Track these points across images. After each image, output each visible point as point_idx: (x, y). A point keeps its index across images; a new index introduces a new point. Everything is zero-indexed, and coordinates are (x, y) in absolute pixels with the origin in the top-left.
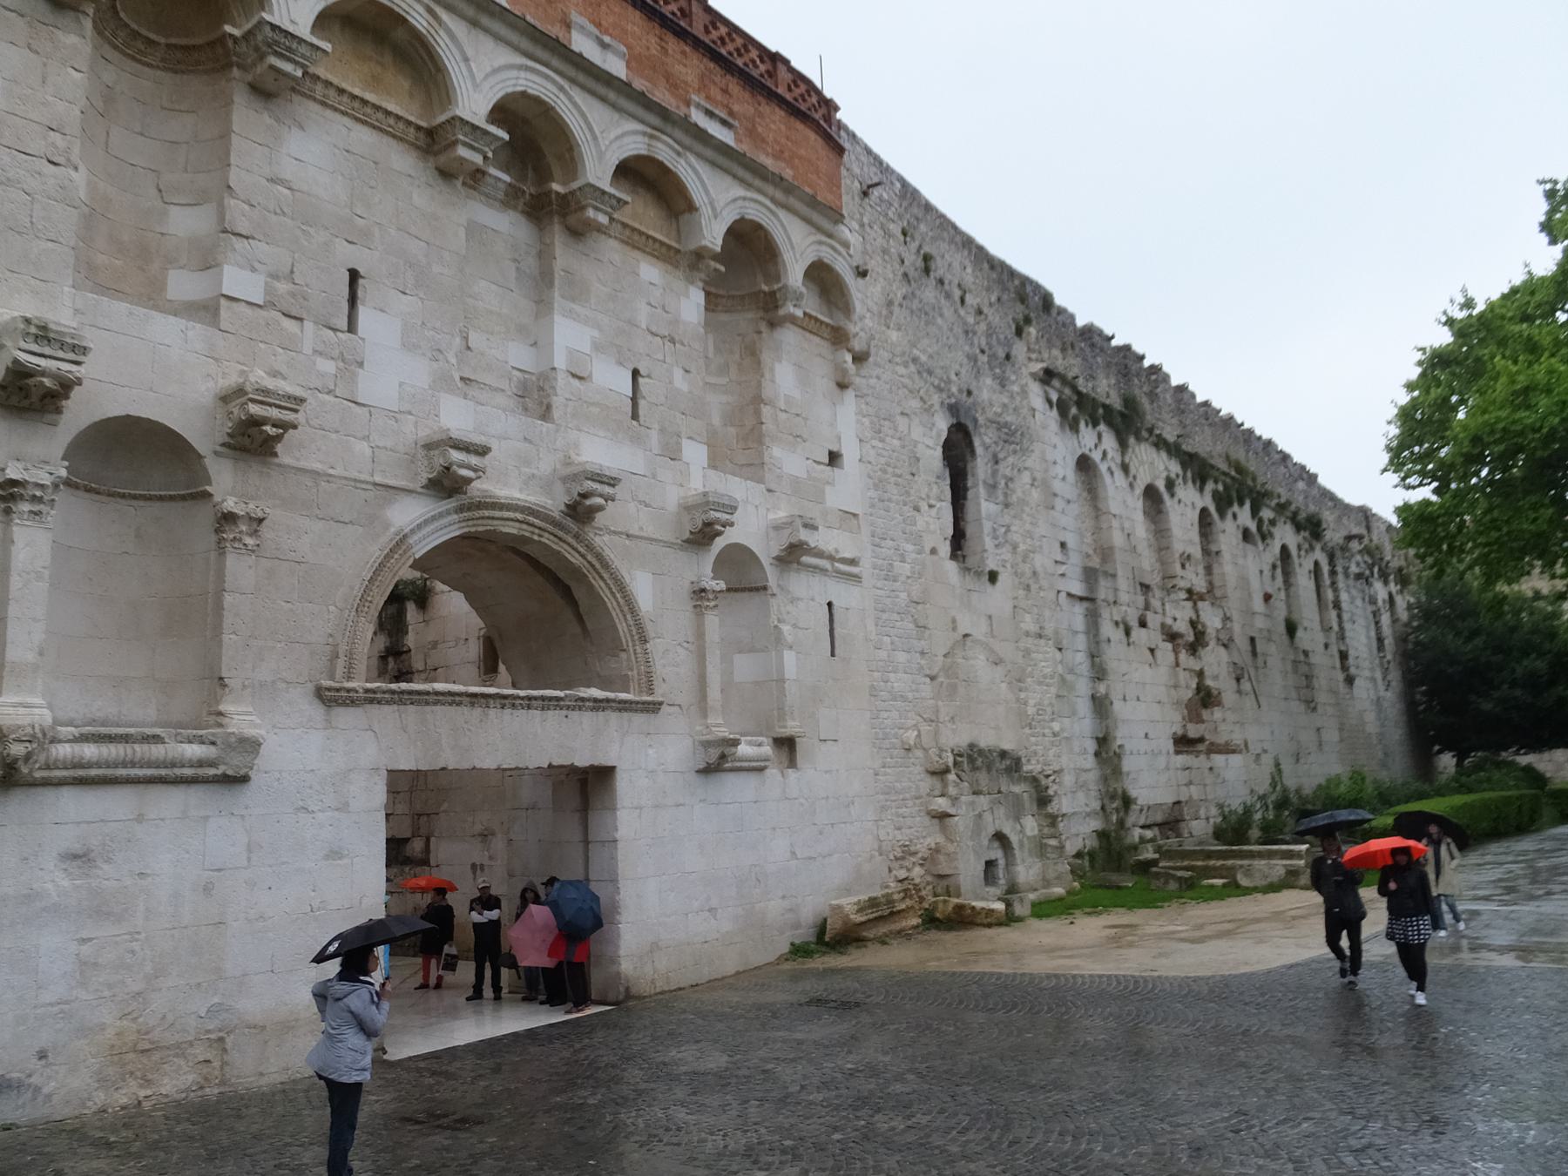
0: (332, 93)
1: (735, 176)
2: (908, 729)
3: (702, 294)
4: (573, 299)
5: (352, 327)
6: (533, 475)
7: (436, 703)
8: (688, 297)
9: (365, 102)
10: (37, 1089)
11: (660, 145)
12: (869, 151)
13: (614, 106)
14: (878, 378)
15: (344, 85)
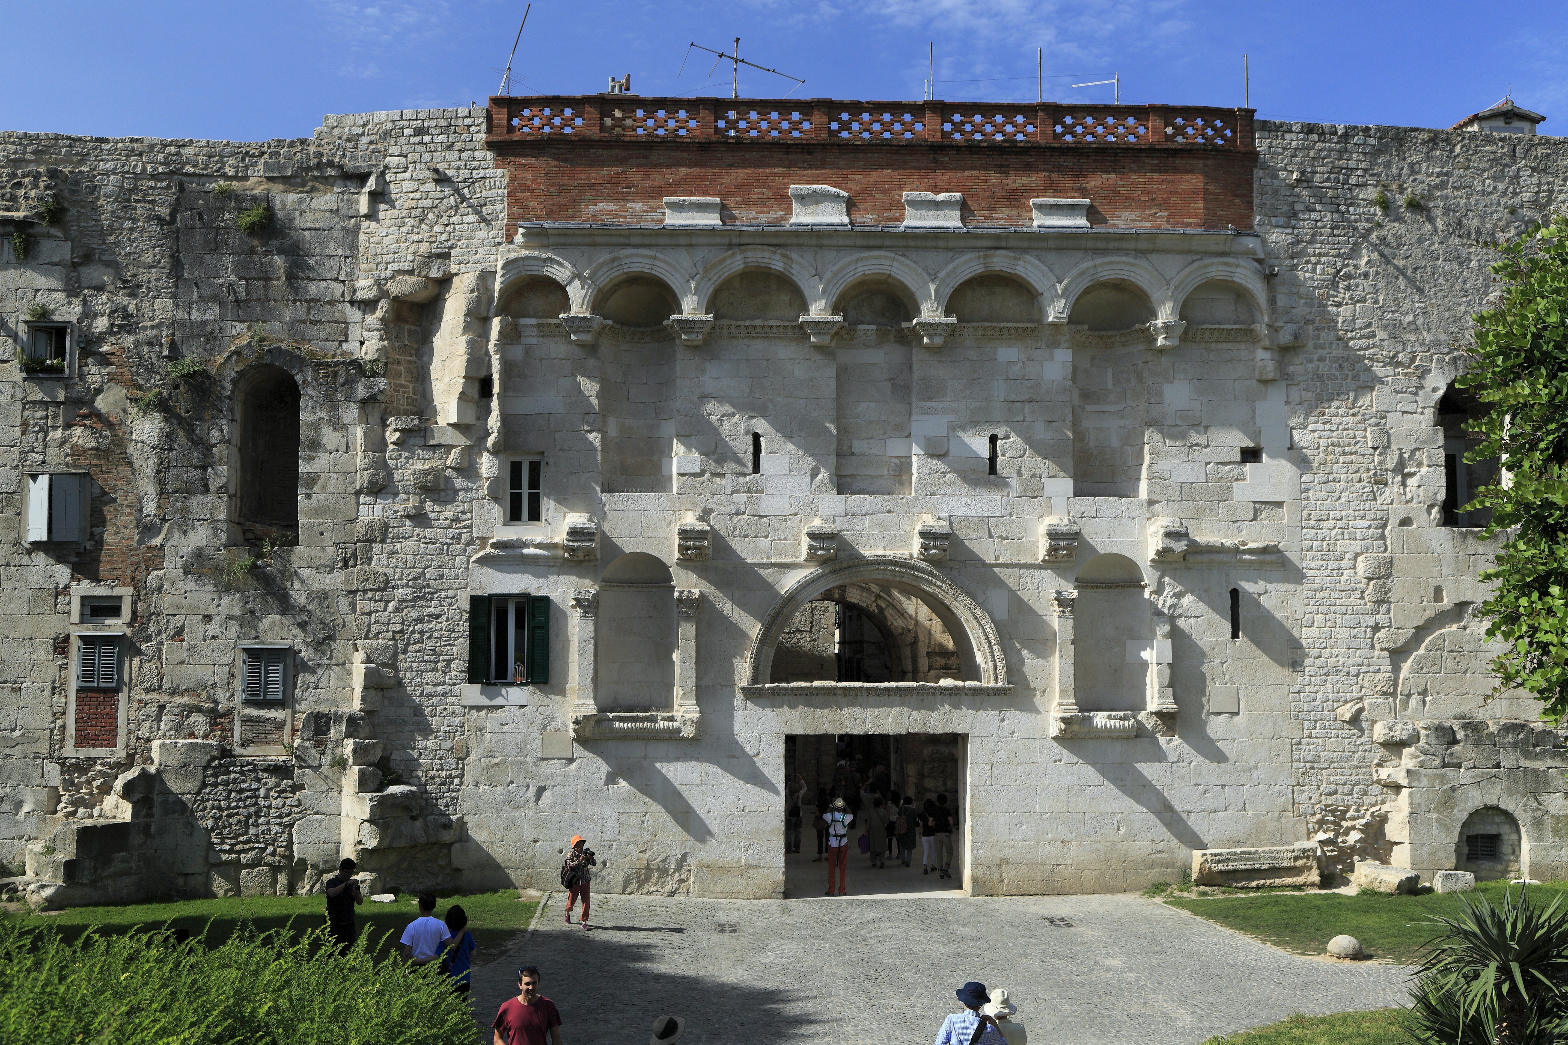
0: (733, 330)
1: (1086, 250)
2: (1346, 702)
3: (1069, 352)
4: (930, 399)
5: (756, 468)
6: (896, 535)
7: (818, 695)
8: (1052, 360)
9: (755, 327)
10: (603, 878)
11: (995, 260)
12: (1309, 129)
13: (947, 249)
14: (1321, 359)
15: (739, 323)
